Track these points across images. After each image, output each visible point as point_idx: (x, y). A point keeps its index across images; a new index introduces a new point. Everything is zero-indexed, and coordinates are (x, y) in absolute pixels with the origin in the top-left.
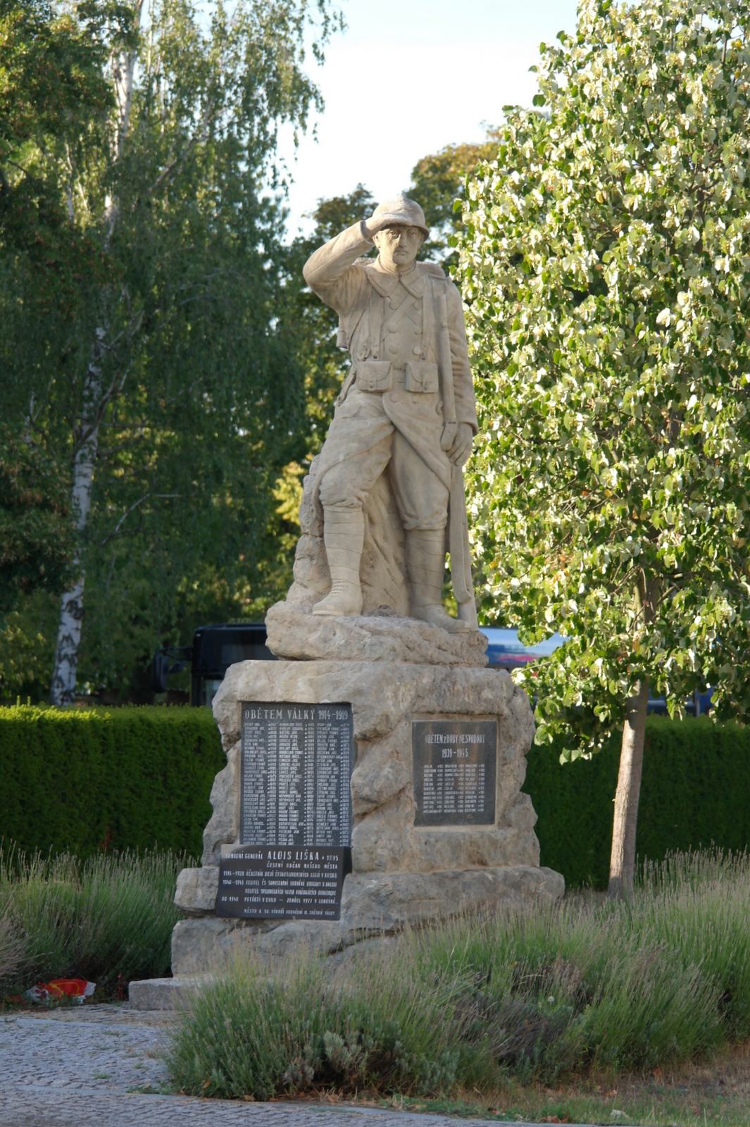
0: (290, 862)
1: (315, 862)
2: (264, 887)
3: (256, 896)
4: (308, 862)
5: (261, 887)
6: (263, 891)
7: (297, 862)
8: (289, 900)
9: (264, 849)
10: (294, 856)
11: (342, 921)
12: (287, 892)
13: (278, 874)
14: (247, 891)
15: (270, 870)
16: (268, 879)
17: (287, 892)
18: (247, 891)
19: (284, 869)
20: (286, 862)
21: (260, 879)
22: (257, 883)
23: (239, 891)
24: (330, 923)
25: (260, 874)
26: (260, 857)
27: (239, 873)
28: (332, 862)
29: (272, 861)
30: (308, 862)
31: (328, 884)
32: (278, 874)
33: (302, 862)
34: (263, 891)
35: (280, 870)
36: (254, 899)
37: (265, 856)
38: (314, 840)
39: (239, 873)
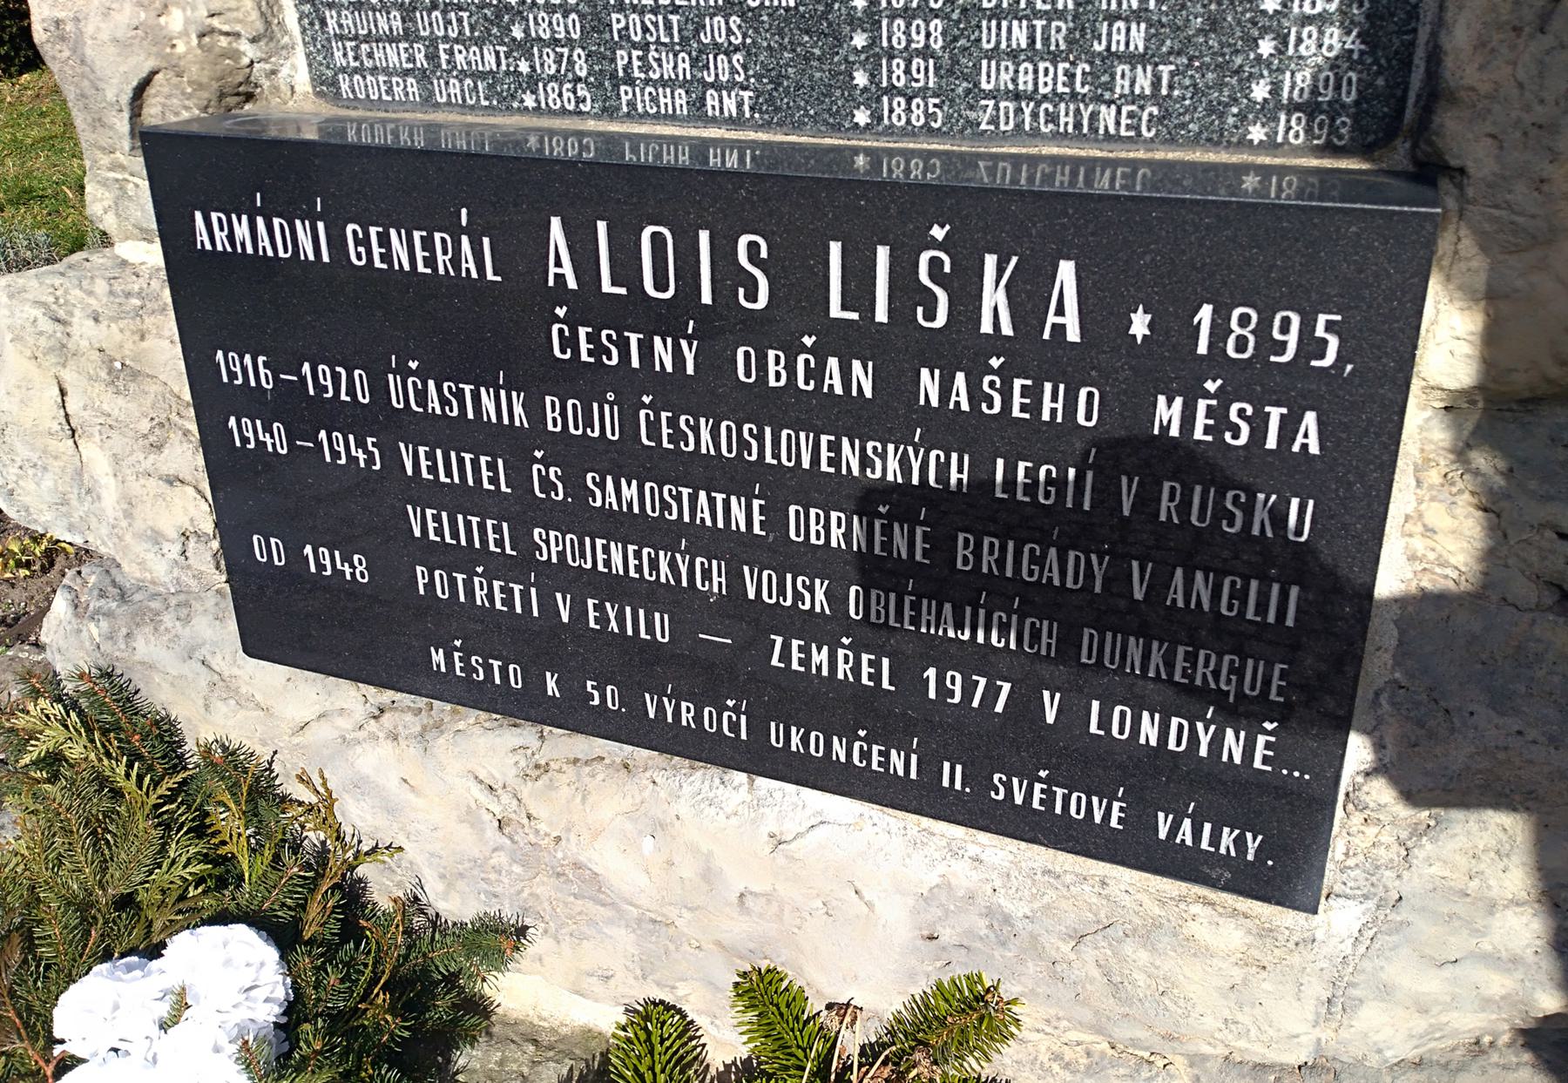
0: (760, 330)
1: (1033, 353)
2: (554, 517)
3: (499, 567)
4: (961, 348)
5: (524, 512)
6: (551, 545)
7: (845, 342)
8: (788, 654)
9: (503, 187)
10: (798, 279)
11: (1338, 919)
12: (758, 584)
13: (656, 427)
14: (423, 522)
15: (583, 382)
16: (577, 456)
17: (758, 584)
18: (423, 522)
19: (710, 393)
20: (721, 327)
21: (513, 446)
22: (490, 474)
23: (369, 511)
24: (1221, 924)
25: (499, 406)
26: (474, 259)
27: (319, 377)
28: (1256, 380)
29: (588, 306)
30: (961, 348)
31: (1193, 590)
32: (656, 427)
33: (897, 350)
34: (551, 545)
35: (674, 392)
36: (486, 592)
37: (524, 253)
38: (957, 68)
39: (319, 377)
